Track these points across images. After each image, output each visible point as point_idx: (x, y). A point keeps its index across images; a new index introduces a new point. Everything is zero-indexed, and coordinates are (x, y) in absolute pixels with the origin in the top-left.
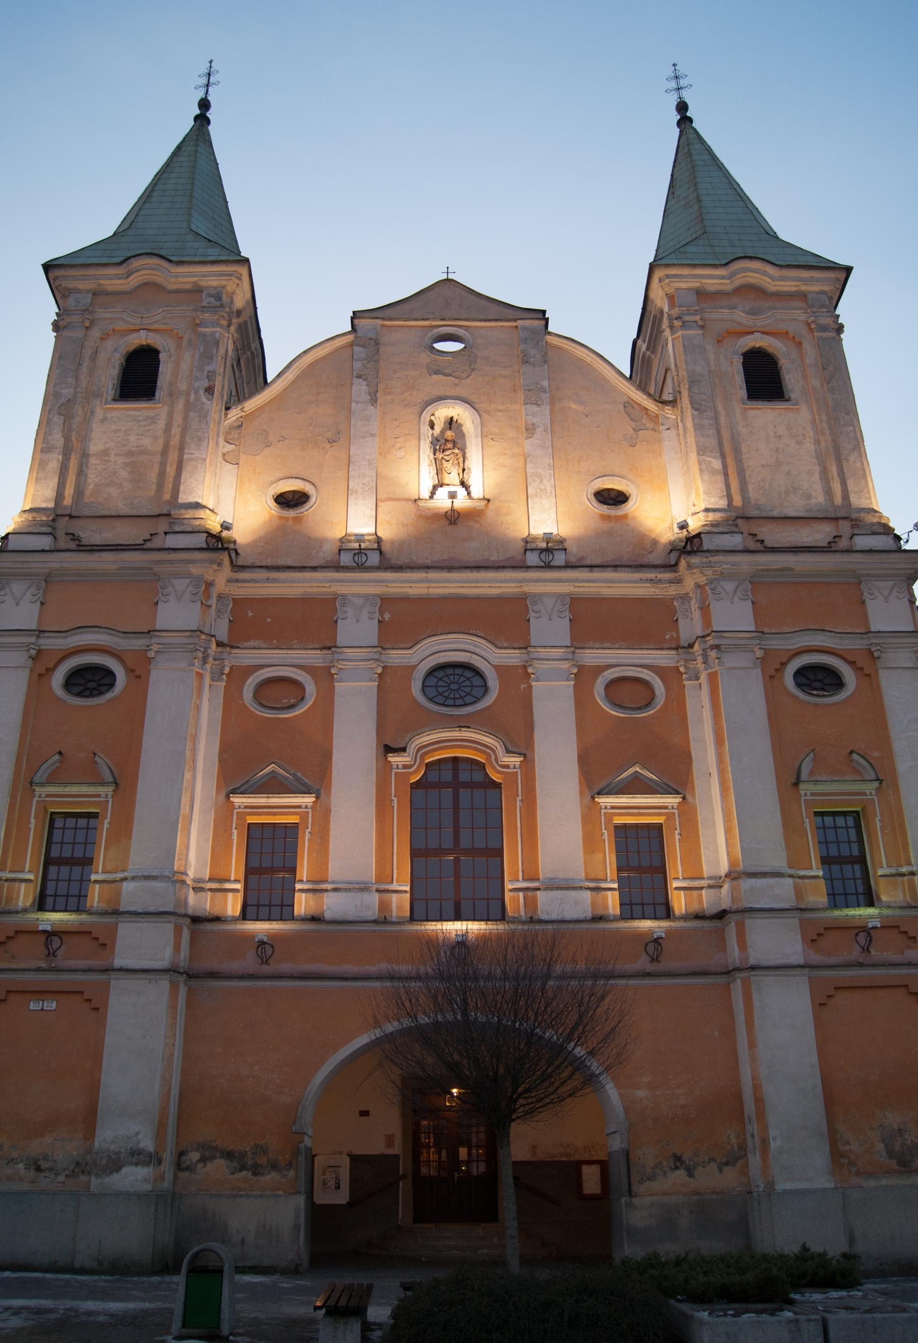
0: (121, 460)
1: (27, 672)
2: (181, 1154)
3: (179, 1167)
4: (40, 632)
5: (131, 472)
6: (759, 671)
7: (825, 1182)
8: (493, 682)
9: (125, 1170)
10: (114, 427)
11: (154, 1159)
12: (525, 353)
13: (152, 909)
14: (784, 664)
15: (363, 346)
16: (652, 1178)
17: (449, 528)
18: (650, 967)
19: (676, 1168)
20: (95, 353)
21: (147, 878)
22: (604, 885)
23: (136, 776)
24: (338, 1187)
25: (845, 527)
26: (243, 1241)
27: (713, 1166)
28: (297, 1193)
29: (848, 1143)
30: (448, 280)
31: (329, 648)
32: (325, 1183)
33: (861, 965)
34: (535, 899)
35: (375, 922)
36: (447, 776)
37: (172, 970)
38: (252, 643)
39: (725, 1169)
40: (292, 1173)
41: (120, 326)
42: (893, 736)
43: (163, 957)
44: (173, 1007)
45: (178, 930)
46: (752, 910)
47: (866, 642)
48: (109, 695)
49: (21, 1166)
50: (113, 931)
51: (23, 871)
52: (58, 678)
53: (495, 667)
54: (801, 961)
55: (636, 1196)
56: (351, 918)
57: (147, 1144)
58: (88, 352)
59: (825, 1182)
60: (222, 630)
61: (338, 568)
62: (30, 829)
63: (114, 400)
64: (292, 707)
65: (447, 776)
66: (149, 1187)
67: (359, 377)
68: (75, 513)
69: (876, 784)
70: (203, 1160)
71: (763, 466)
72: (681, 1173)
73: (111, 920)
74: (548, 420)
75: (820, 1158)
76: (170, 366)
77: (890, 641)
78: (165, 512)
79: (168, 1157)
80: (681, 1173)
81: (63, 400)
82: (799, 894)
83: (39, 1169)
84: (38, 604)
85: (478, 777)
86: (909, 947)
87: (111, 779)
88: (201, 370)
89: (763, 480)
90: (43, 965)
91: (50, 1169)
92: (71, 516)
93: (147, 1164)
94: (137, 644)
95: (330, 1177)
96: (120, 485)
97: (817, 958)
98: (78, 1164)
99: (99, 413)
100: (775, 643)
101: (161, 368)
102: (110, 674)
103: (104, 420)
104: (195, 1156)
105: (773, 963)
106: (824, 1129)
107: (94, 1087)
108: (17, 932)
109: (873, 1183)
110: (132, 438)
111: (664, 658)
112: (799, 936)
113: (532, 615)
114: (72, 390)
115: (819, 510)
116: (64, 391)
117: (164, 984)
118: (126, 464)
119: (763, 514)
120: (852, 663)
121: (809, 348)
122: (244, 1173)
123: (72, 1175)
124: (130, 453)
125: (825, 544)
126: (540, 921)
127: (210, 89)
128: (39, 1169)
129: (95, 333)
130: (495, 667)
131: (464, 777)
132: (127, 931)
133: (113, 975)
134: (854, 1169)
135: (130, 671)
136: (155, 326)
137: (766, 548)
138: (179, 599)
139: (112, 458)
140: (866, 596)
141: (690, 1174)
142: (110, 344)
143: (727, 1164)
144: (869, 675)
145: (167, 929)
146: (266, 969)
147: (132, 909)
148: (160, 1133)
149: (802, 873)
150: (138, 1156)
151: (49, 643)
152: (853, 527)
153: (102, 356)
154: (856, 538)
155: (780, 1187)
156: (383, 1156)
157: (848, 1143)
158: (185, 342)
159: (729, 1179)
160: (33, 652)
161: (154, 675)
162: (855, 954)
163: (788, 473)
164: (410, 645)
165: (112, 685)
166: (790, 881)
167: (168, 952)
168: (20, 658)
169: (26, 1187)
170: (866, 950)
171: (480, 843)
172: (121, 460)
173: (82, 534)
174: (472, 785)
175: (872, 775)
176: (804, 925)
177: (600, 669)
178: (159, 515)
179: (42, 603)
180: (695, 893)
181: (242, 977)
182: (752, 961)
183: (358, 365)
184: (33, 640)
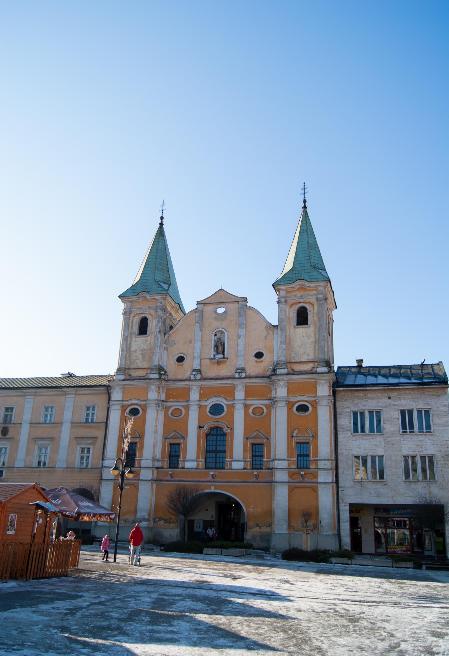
0: (140, 352)
2: (155, 519)
3: (154, 522)
4: (123, 401)
5: (142, 356)
6: (286, 407)
7: (286, 532)
8: (225, 409)
9: (142, 522)
10: (138, 343)
11: (148, 520)
12: (239, 313)
13: (147, 466)
14: (294, 405)
15: (198, 313)
16: (252, 528)
17: (218, 366)
18: (256, 481)
19: (257, 527)
20: (132, 322)
21: (147, 459)
22: (247, 460)
23: (144, 435)
24: (200, 528)
25: (316, 364)
26: (166, 538)
27: (265, 527)
28: (178, 528)
29: (293, 524)
30: (222, 289)
31: (188, 401)
32: (197, 526)
33: (301, 482)
34: (231, 463)
35: (196, 469)
36: (215, 432)
38: (171, 400)
39: (268, 528)
40: (177, 524)
41: (138, 312)
42: (318, 424)
43: (150, 477)
44: (152, 488)
45: (153, 471)
46: (277, 468)
47: (315, 398)
48: (138, 416)
49: (123, 521)
50: (140, 471)
53: (226, 405)
54: (287, 481)
55: (248, 532)
56: (190, 468)
57: (147, 517)
58: (131, 321)
59: (286, 532)
60: (163, 397)
61: (190, 380)
63: (138, 335)
64: (179, 416)
65: (215, 432)
66: (147, 526)
67: (197, 323)
68: (130, 368)
69: (312, 437)
70: (159, 521)
71: (297, 346)
72: (258, 528)
73: (139, 469)
74: (244, 333)
75: (285, 526)
76: (151, 324)
77: (321, 398)
78: (149, 367)
79: (151, 520)
80: (258, 528)
81: (125, 336)
82: (289, 465)
83: (126, 522)
84: (122, 394)
85: (222, 433)
86: (314, 479)
87: (139, 436)
88: (158, 326)
89: (297, 351)
91: (128, 522)
92: (129, 369)
93: (146, 521)
94: (144, 403)
95: (198, 525)
96: (140, 359)
97: (291, 480)
98: (133, 521)
99: (134, 339)
100: (292, 399)
101: (148, 325)
102: (138, 410)
103: (135, 341)
104: (157, 520)
105: (280, 481)
106: (287, 520)
107: (136, 505)
109: (297, 533)
110: (142, 346)
111: (267, 402)
112: (287, 475)
113: (235, 391)
114: (127, 333)
115: (310, 359)
116: (125, 334)
118: (141, 354)
119: (295, 361)
120: (311, 404)
121: (316, 307)
122: (167, 524)
123: (132, 523)
124: (142, 351)
125: (310, 370)
126: (232, 469)
128: (126, 522)
129: (132, 315)
130: (226, 405)
131: (219, 432)
133: (140, 481)
134: (293, 529)
135: (142, 409)
137: (294, 371)
138: (153, 391)
139: (137, 352)
140: (317, 386)
141: (260, 528)
142: (136, 318)
143: (268, 526)
144: (315, 407)
145: (150, 471)
146: (172, 479)
147: (143, 466)
148: (149, 515)
149: (291, 459)
150: (145, 520)
151: (125, 403)
152: (318, 364)
153: (134, 322)
154: (317, 368)
155: (276, 532)
156: (211, 521)
157: (293, 524)
158: (154, 317)
159: (267, 530)
160: (121, 406)
162: (301, 479)
163: (304, 348)
164: (206, 400)
165: (139, 412)
166: (287, 462)
168: (119, 407)
169: (123, 525)
170: (303, 479)
171: (221, 449)
172: (140, 352)
173: (132, 374)
174: (221, 435)
175: (311, 435)
176: (289, 472)
177: (251, 405)
178: (148, 368)
180: (268, 463)
181: (167, 481)
182: (276, 481)
183: (197, 319)
184: (121, 403)
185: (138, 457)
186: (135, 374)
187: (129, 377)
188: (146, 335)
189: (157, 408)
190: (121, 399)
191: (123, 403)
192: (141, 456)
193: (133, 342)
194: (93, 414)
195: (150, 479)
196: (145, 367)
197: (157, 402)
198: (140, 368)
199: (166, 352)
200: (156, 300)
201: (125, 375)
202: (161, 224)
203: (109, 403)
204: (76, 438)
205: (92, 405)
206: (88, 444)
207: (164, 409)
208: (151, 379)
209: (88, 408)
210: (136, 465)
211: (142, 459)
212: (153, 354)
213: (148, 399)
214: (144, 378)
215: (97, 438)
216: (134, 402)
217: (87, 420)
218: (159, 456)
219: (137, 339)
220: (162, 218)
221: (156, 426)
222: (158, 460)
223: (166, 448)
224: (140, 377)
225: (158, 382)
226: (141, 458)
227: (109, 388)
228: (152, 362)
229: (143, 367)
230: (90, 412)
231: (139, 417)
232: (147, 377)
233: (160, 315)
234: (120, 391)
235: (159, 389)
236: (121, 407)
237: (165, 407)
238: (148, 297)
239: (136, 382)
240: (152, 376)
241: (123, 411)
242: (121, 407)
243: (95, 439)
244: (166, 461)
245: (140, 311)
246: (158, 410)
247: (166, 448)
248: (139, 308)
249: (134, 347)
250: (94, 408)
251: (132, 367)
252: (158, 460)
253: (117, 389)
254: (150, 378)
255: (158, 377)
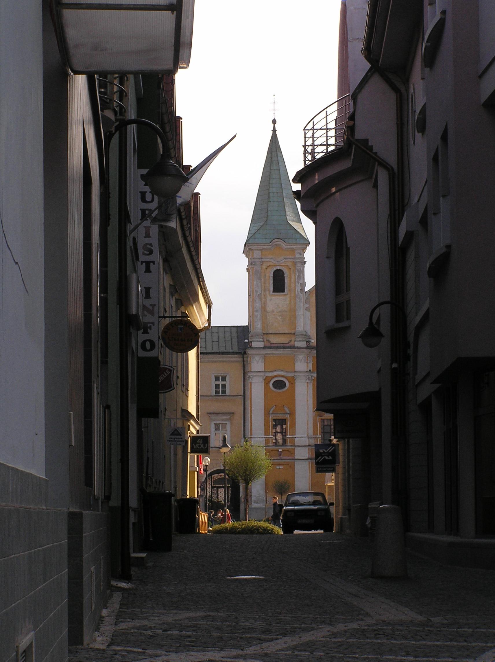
1: (263, 383)
4: (265, 372)
5: (281, 318)
13: (303, 445)
37: (308, 459)
41: (272, 264)
43: (307, 456)
48: (285, 389)
51: (270, 435)
52: (271, 385)
62: (270, 425)
78: (293, 333)
81: (258, 293)
84: (263, 364)
90: (279, 458)
99: (269, 298)
108: (272, 451)
117: (307, 462)
124: (281, 312)
127: (276, 112)
129: (264, 267)
132: (298, 451)
135: (289, 382)
136: (283, 264)
145: (306, 449)
151: (268, 374)
161: (296, 383)
167: (307, 455)
168: (261, 379)
173: (270, 339)
179: (264, 363)
184: (263, 374)
185: (289, 435)
186: (275, 340)
187: (268, 345)
188: (284, 293)
189: (307, 381)
190: (263, 370)
191: (265, 374)
192: (294, 433)
193: (268, 301)
194: (224, 386)
195: (307, 458)
196: (286, 332)
197: (307, 374)
198: (280, 334)
199: (308, 313)
200: (294, 250)
201: (263, 341)
202: (274, 131)
203: (244, 373)
204: (208, 413)
205: (223, 375)
206: (223, 420)
207: (312, 381)
208: (297, 348)
209: (217, 379)
210: (289, 443)
211: (295, 437)
212: (295, 316)
213: (296, 371)
214: (287, 345)
215: (233, 413)
216: (279, 374)
217: (217, 392)
218: (311, 433)
219: (273, 298)
220: (274, 122)
221: (308, 400)
222: (312, 438)
223: (318, 424)
224: (282, 344)
225: (307, 351)
226: (294, 436)
227: (245, 356)
228: (296, 326)
229: (283, 332)
230: (220, 383)
231: (287, 390)
232: (292, 343)
233: (300, 269)
234: (260, 361)
235: (307, 359)
236: (264, 379)
237: (313, 378)
238: (284, 245)
239: (280, 351)
240: (297, 344)
241: (267, 384)
242: (264, 379)
243: (232, 415)
244: (319, 437)
245: (273, 261)
246: (308, 383)
247: (318, 424)
248: (272, 258)
249: (270, 307)
250: (224, 379)
251: (270, 332)
252: (312, 438)
253: (257, 358)
254: (296, 346)
255: (306, 346)
